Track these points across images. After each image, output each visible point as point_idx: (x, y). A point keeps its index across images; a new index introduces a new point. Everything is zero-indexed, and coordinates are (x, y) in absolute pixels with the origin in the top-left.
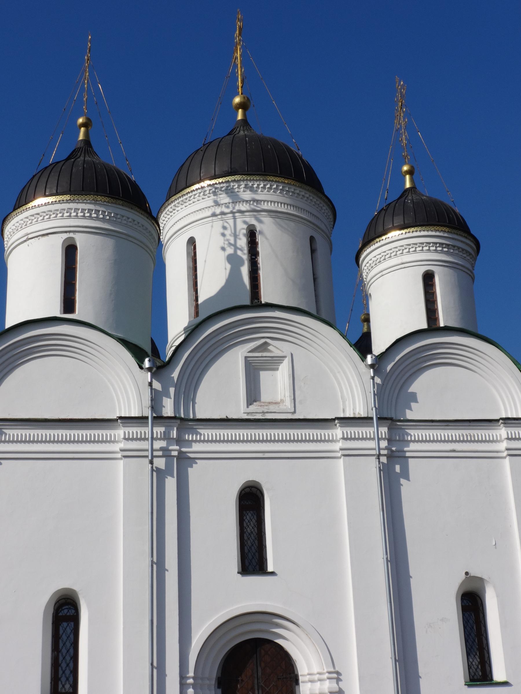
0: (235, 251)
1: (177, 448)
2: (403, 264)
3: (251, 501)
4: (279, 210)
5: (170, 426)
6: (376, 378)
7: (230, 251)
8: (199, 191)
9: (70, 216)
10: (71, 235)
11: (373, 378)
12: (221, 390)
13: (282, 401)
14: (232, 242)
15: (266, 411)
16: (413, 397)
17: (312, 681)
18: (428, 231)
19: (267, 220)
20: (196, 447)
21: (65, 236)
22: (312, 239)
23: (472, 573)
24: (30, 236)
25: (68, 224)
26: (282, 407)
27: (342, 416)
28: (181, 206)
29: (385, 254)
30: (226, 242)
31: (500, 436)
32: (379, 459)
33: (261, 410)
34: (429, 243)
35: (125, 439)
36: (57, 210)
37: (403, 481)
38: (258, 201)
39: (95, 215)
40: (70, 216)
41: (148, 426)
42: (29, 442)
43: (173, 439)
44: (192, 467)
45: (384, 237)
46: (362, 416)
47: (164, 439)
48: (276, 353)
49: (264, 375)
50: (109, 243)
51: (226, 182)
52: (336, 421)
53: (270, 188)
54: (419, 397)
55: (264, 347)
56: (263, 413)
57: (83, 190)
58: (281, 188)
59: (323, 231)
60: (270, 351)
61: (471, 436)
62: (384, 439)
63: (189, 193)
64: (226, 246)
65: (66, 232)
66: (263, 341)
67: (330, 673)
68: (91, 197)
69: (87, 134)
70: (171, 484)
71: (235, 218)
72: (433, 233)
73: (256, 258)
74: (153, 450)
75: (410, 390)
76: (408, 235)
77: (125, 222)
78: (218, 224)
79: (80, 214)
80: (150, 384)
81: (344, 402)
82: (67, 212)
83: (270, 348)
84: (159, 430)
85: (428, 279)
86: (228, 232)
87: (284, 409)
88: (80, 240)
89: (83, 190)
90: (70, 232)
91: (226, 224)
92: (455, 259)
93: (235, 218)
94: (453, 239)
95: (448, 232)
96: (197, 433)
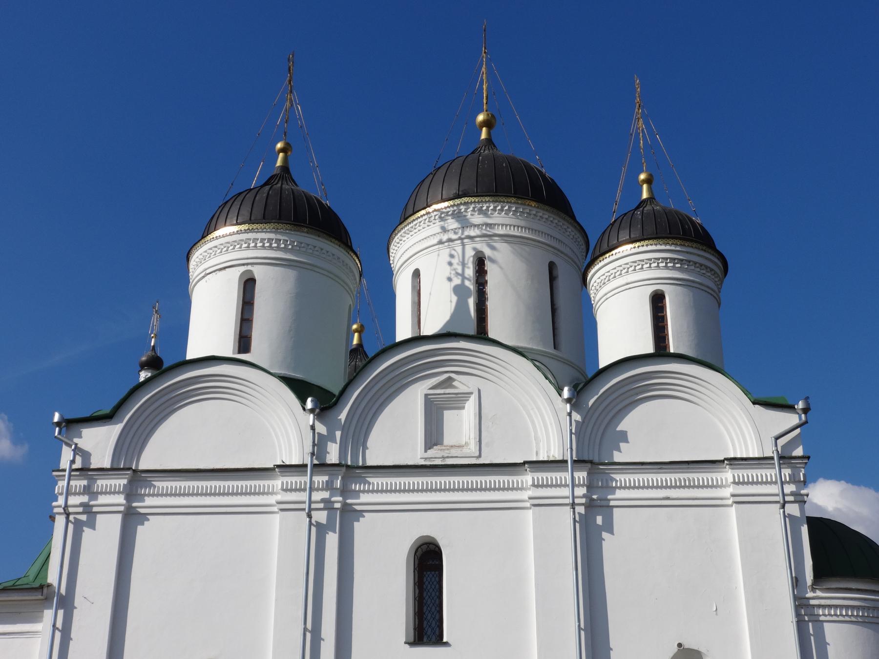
0: (463, 281)
1: (340, 499)
2: (627, 284)
3: (427, 561)
6: (574, 414)
7: (457, 281)
8: (424, 218)
9: (248, 247)
10: (249, 268)
11: (570, 414)
12: (397, 432)
13: (467, 444)
14: (460, 271)
15: (446, 455)
16: (623, 437)
18: (656, 245)
20: (364, 498)
21: (243, 269)
22: (552, 266)
23: (687, 645)
24: (208, 271)
25: (246, 256)
26: (465, 451)
27: (535, 459)
28: (408, 236)
30: (453, 272)
31: (726, 479)
32: (574, 509)
33: (440, 454)
34: (658, 259)
35: (283, 489)
37: (605, 535)
38: (490, 225)
40: (248, 247)
42: (180, 495)
43: (337, 489)
44: (358, 521)
45: (607, 255)
47: (326, 490)
48: (462, 389)
49: (448, 415)
50: (291, 274)
51: (452, 206)
53: (502, 210)
54: (630, 437)
56: (443, 458)
57: (264, 218)
59: (566, 255)
60: (455, 387)
61: (689, 480)
62: (582, 486)
63: (414, 220)
64: (452, 276)
65: (243, 265)
66: (446, 376)
68: (272, 225)
69: (285, 159)
72: (663, 247)
74: (310, 502)
75: (620, 428)
76: (637, 250)
77: (311, 251)
78: (445, 252)
80: (313, 428)
84: (321, 479)
85: (657, 301)
86: (455, 261)
87: (468, 454)
88: (258, 272)
90: (247, 264)
91: (453, 252)
92: (690, 276)
93: (463, 245)
94: (687, 253)
95: (681, 245)
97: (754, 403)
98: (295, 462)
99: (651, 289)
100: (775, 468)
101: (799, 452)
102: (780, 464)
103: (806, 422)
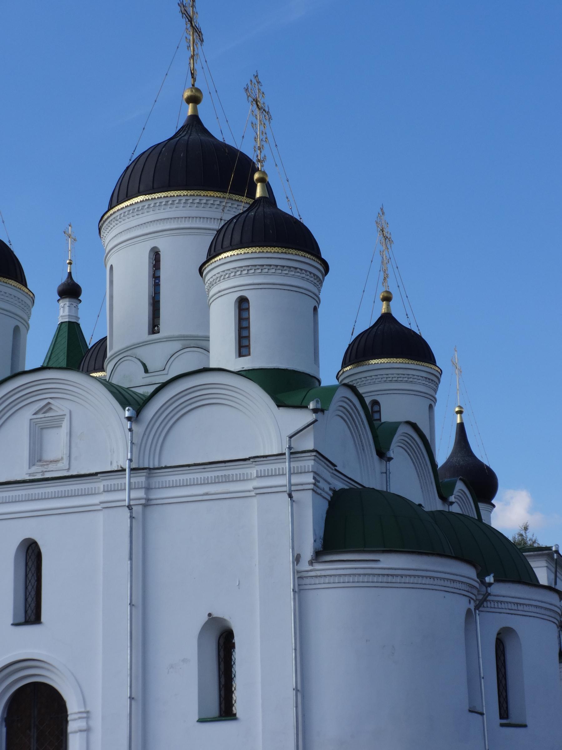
15: (45, 470)
23: (215, 615)
83: (53, 407)
99: (236, 296)
100: (285, 462)
102: (290, 458)
103: (316, 421)
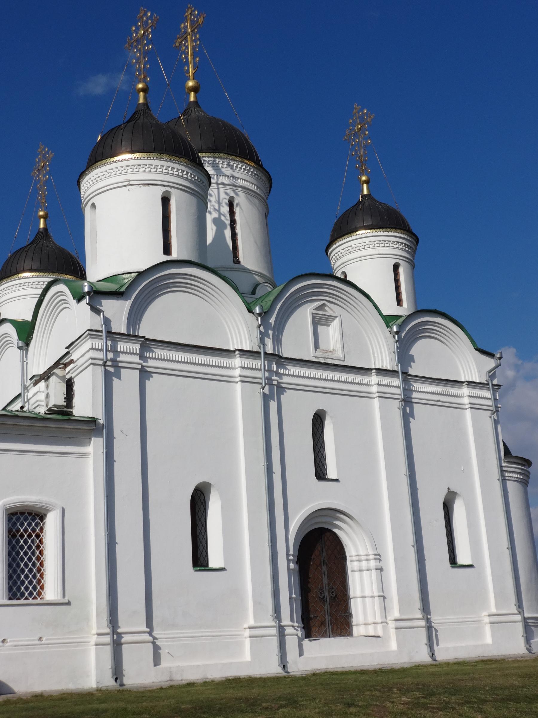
4: (249, 188)
5: (271, 361)
12: (297, 337)
14: (217, 208)
15: (327, 357)
17: (359, 561)
19: (242, 195)
20: (285, 379)
21: (164, 189)
23: (451, 489)
24: (131, 183)
29: (365, 244)
30: (212, 207)
36: (158, 166)
37: (411, 419)
38: (234, 177)
39: (181, 174)
41: (261, 360)
43: (273, 371)
44: (283, 394)
46: (389, 369)
49: (320, 328)
52: (373, 371)
53: (245, 169)
55: (321, 308)
56: (325, 358)
58: (252, 170)
60: (325, 311)
64: (212, 210)
65: (164, 186)
66: (322, 302)
67: (375, 555)
68: (184, 160)
70: (273, 405)
71: (218, 188)
73: (234, 224)
75: (410, 353)
79: (164, 171)
81: (374, 357)
82: (166, 169)
83: (326, 308)
89: (175, 153)
90: (167, 186)
93: (218, 188)
96: (286, 369)
97: (476, 349)
98: (247, 347)
101: (495, 382)
